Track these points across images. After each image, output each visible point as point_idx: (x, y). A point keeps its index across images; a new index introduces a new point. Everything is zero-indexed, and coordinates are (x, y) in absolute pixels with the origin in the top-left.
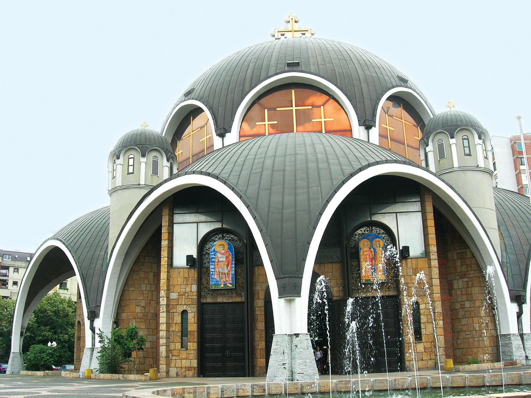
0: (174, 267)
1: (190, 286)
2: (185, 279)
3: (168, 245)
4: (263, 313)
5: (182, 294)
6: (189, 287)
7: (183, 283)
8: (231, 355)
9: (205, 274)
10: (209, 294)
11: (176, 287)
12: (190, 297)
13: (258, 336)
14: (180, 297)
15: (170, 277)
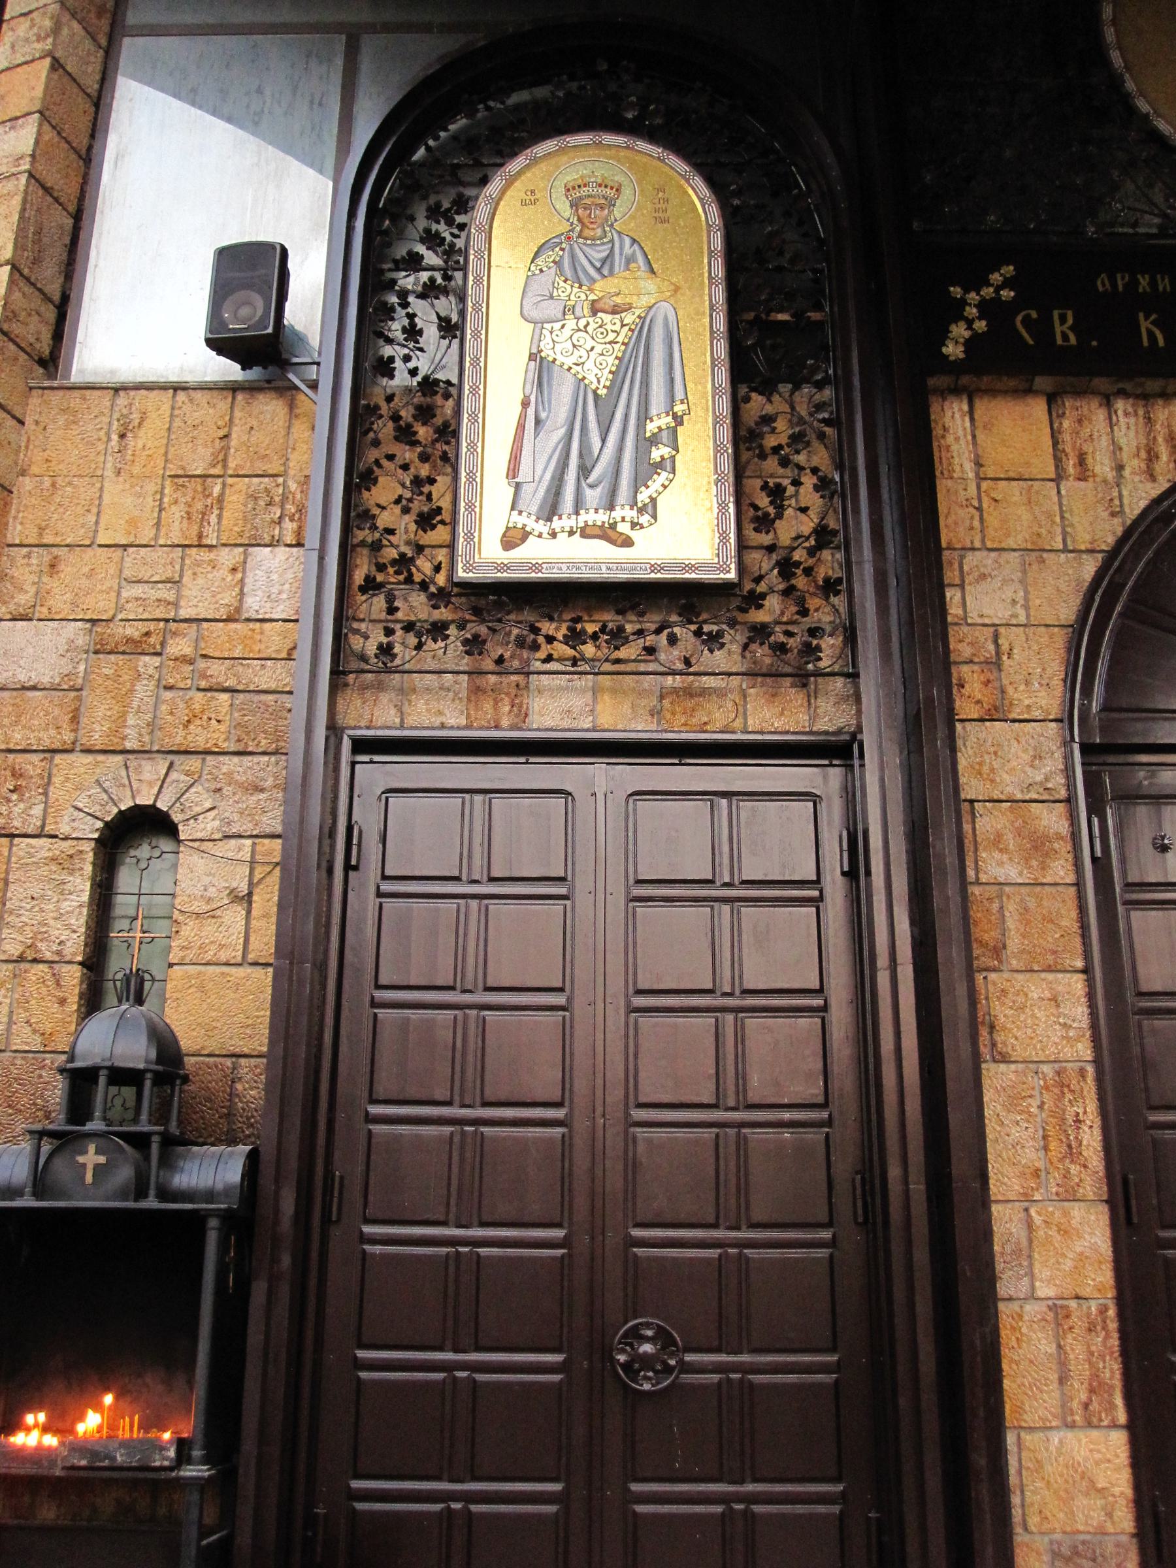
0: (75, 377)
1: (229, 557)
2: (178, 487)
3: (33, 156)
4: (1061, 870)
5: (136, 635)
6: (223, 572)
7: (158, 524)
8: (686, 1368)
9: (405, 435)
10: (438, 630)
11: (66, 570)
12: (218, 671)
13: (1016, 1133)
14: (108, 665)
15: (23, 473)
